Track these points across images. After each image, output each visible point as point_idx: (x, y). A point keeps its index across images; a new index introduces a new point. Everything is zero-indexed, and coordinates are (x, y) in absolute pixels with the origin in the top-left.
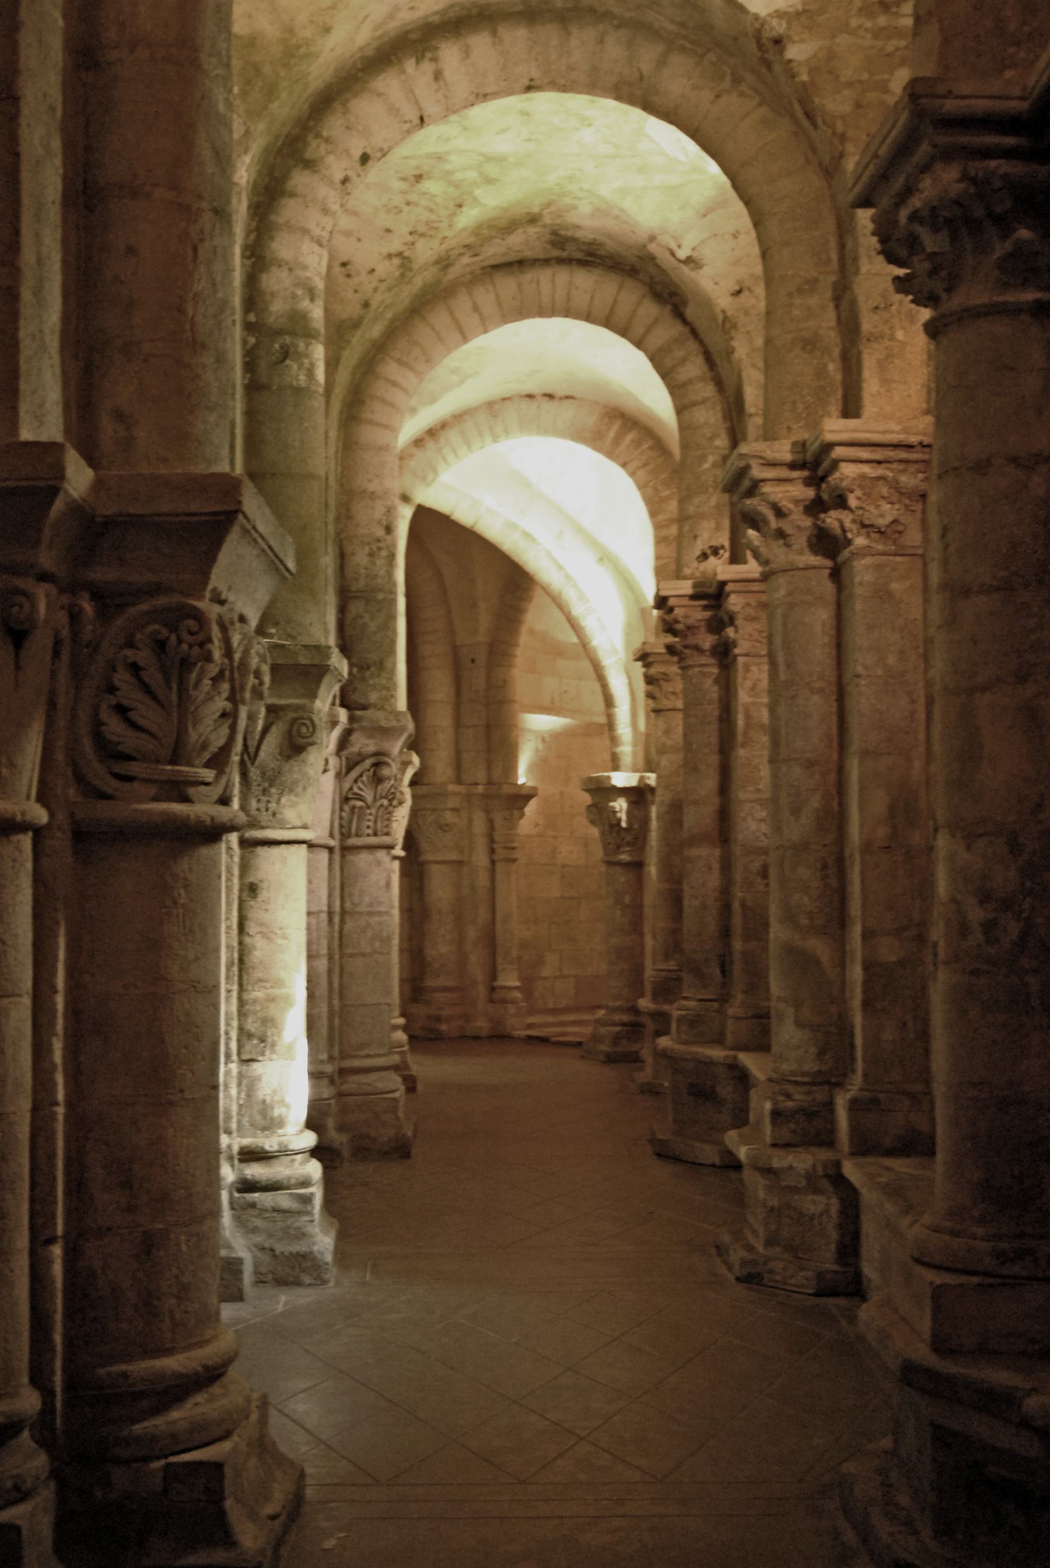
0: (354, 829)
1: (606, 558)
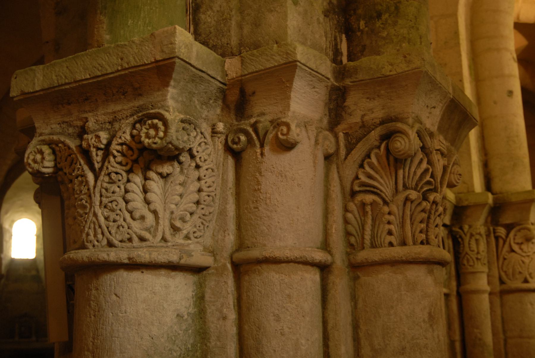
0: (367, 237)
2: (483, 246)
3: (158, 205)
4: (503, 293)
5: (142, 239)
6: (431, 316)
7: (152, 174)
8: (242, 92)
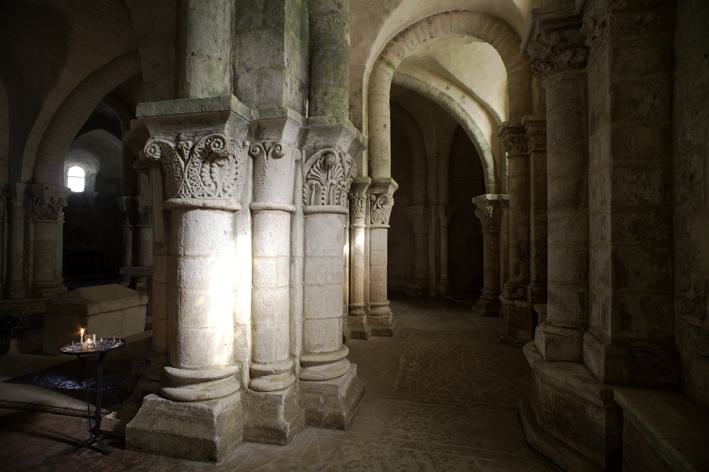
0: (312, 200)
1: (484, 106)
2: (364, 205)
3: (217, 179)
4: (371, 229)
5: (209, 195)
6: (338, 237)
7: (214, 164)
8: (259, 126)
